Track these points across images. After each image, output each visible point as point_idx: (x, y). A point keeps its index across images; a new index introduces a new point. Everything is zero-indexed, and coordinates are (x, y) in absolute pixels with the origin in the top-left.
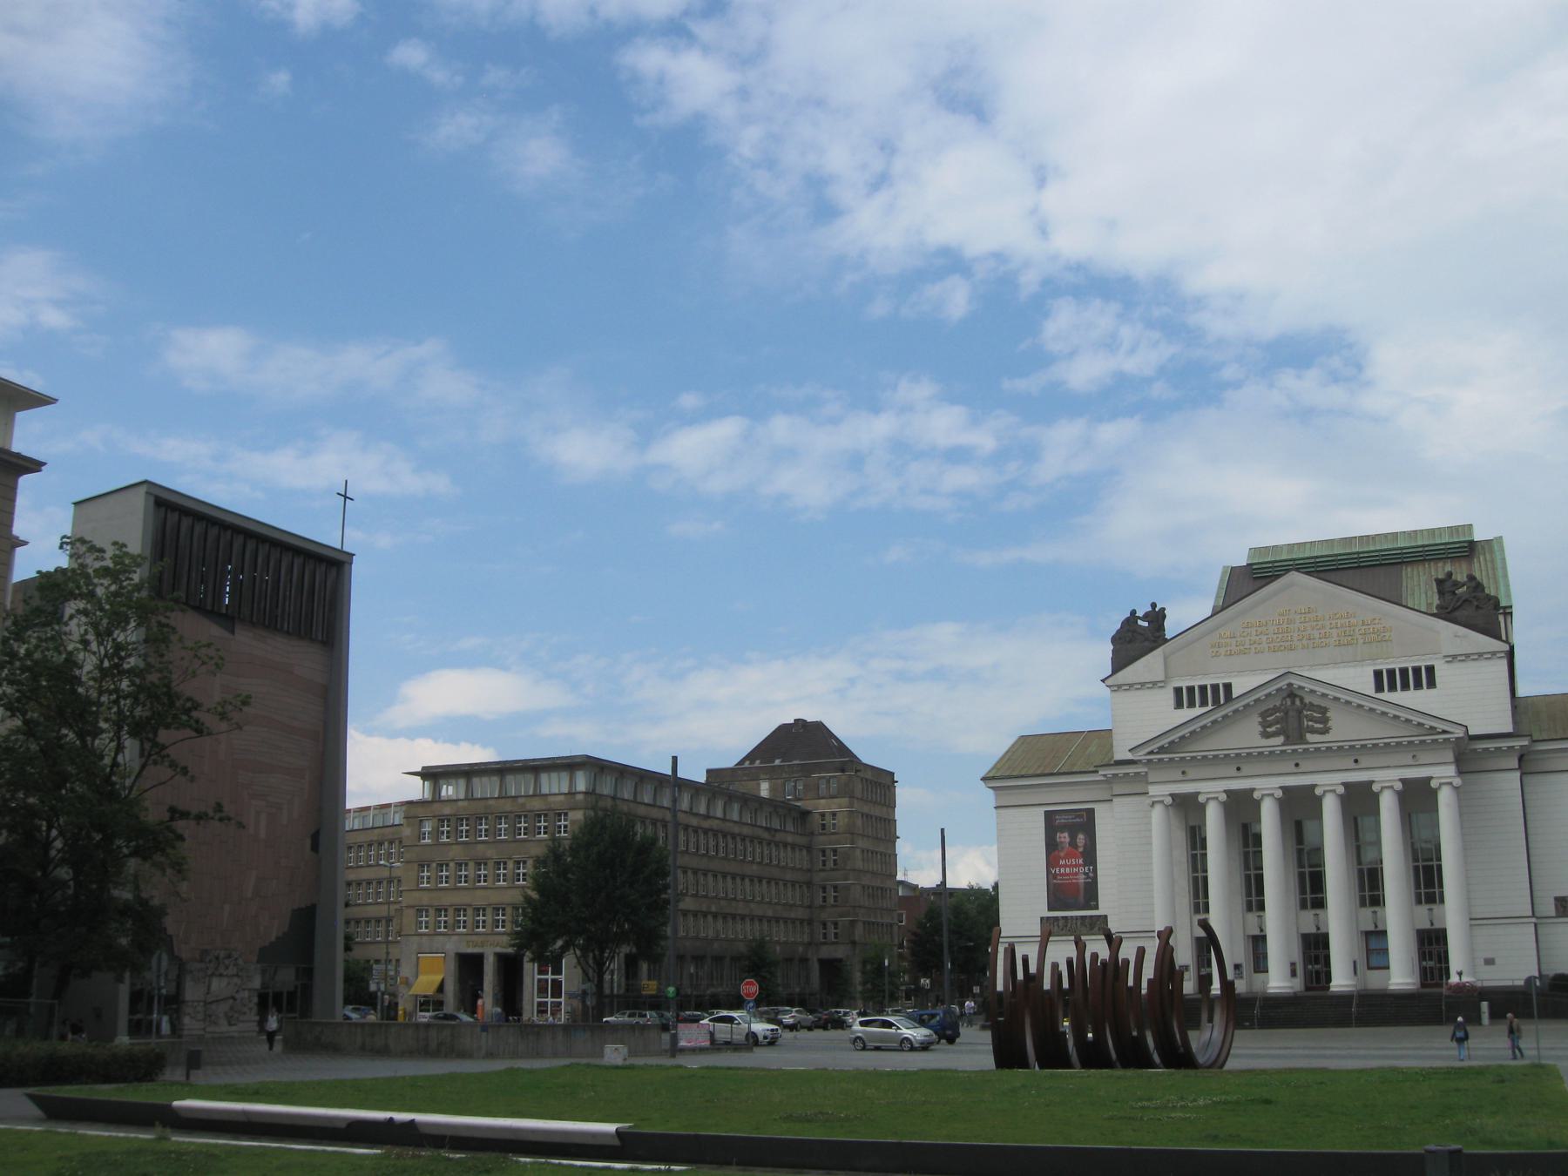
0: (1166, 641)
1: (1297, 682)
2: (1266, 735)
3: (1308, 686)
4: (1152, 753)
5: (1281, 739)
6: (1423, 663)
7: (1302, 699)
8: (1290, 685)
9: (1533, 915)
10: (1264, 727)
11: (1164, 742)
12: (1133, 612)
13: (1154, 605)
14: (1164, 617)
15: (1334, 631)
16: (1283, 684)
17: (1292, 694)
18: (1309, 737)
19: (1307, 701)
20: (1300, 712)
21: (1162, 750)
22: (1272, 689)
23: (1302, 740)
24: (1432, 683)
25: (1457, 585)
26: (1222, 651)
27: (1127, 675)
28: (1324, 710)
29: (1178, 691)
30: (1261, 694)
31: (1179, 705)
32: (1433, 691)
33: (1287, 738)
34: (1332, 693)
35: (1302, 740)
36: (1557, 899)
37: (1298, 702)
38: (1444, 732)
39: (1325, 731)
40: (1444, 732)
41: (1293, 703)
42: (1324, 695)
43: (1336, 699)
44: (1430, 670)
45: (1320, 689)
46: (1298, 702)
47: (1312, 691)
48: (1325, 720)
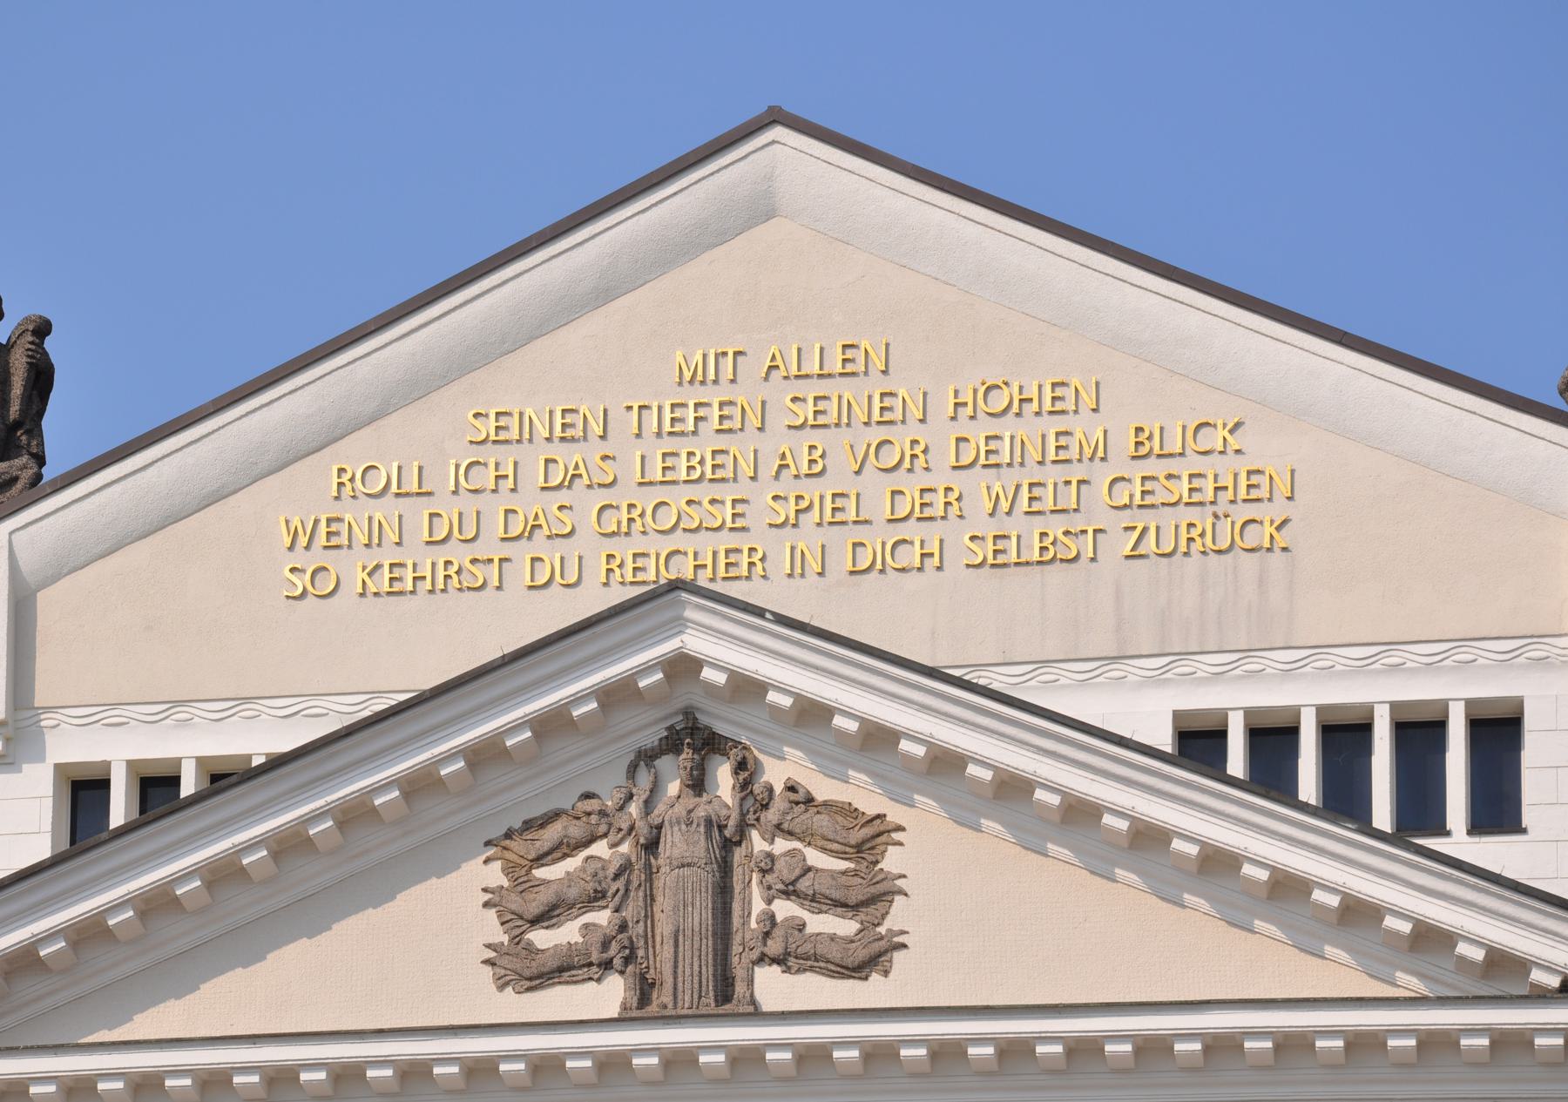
0: (37, 489)
1: (718, 647)
3: (790, 674)
5: (611, 994)
6: (1455, 691)
8: (683, 667)
14: (41, 378)
15: (979, 488)
16: (639, 660)
19: (775, 774)
20: (726, 842)
22: (574, 689)
24: (1497, 809)
26: (351, 569)
28: (866, 840)
30: (507, 719)
33: (644, 989)
34: (923, 722)
35: (725, 995)
37: (723, 778)
39: (868, 961)
41: (698, 783)
42: (877, 740)
43: (945, 764)
44: (1498, 733)
45: (856, 699)
46: (723, 778)
47: (811, 715)
48: (871, 898)
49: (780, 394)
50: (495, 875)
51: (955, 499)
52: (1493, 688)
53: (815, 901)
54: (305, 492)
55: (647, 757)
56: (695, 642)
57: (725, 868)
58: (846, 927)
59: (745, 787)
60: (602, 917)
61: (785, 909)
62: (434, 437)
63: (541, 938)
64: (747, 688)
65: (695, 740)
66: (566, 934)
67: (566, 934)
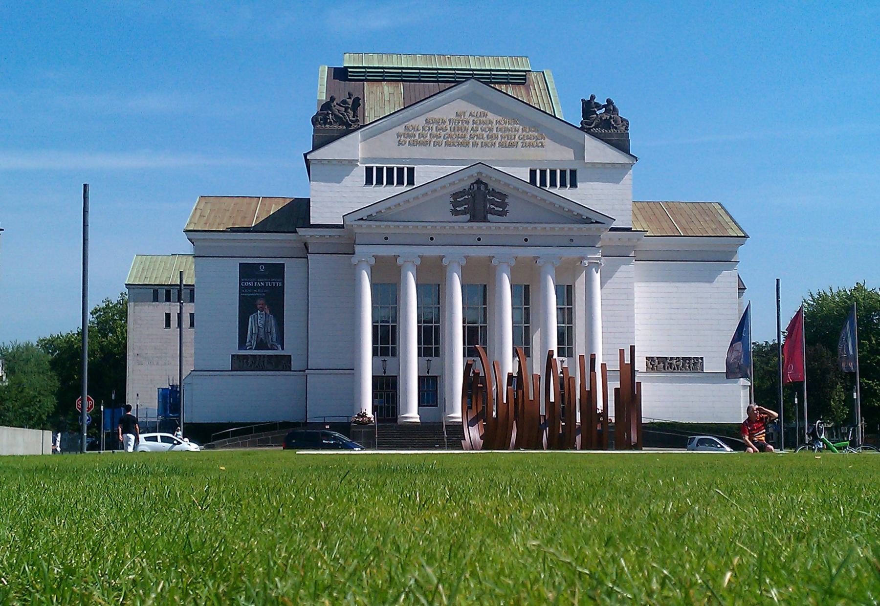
1: (486, 171)
2: (455, 212)
4: (362, 219)
7: (486, 185)
15: (500, 134)
17: (479, 182)
18: (490, 216)
23: (485, 220)
24: (574, 185)
25: (599, 106)
27: (327, 152)
29: (369, 170)
31: (369, 181)
32: (574, 190)
37: (482, 187)
38: (597, 222)
40: (597, 222)
41: (479, 188)
46: (482, 187)
48: (503, 205)
52: (573, 168)
54: (401, 129)
55: (472, 184)
62: (420, 122)
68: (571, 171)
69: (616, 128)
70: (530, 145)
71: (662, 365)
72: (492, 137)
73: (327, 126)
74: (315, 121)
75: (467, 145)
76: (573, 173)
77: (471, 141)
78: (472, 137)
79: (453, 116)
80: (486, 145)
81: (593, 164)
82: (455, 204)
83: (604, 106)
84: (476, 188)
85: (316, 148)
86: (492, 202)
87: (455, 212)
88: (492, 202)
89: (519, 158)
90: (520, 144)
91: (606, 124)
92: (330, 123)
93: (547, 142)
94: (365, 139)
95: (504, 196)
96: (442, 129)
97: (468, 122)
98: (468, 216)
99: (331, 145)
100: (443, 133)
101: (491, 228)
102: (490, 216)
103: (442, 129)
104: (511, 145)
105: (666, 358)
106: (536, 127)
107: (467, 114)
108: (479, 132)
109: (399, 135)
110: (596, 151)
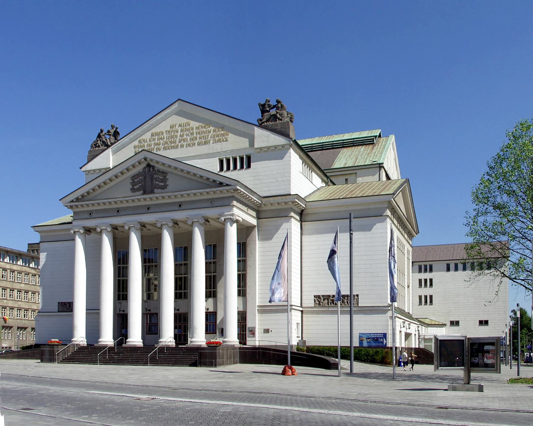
4: (72, 201)
7: (153, 167)
8: (145, 159)
9: (301, 306)
10: (133, 186)
11: (78, 194)
12: (102, 131)
13: (113, 127)
18: (156, 190)
21: (78, 200)
23: (152, 192)
32: (249, 170)
36: (315, 296)
38: (227, 185)
40: (227, 185)
48: (165, 180)
49: (180, 129)
50: (131, 181)
51: (196, 138)
53: (160, 182)
54: (136, 143)
55: (145, 168)
56: (146, 156)
57: (152, 179)
58: (163, 184)
59: (153, 171)
60: (140, 185)
61: (157, 183)
62: (147, 136)
63: (135, 187)
64: (152, 160)
65: (149, 165)
66: (138, 186)
67: (138, 186)
68: (246, 156)
69: (281, 120)
70: (219, 141)
71: (326, 301)
72: (193, 139)
73: (97, 148)
74: (92, 146)
75: (177, 147)
76: (249, 158)
77: (180, 144)
78: (180, 142)
79: (169, 129)
80: (189, 145)
81: (261, 149)
82: (133, 184)
83: (274, 107)
84: (147, 171)
85: (88, 162)
86: (157, 179)
87: (133, 190)
88: (157, 179)
89: (211, 152)
90: (211, 142)
91: (274, 117)
92: (99, 146)
93: (231, 137)
94: (114, 153)
95: (164, 173)
96: (161, 139)
97: (177, 132)
98: (142, 192)
99: (95, 160)
100: (162, 142)
101: (158, 197)
102: (156, 190)
103: (161, 139)
104: (206, 143)
105: (329, 296)
106: (223, 128)
107: (177, 126)
108: (185, 136)
109: (135, 147)
110: (264, 138)
